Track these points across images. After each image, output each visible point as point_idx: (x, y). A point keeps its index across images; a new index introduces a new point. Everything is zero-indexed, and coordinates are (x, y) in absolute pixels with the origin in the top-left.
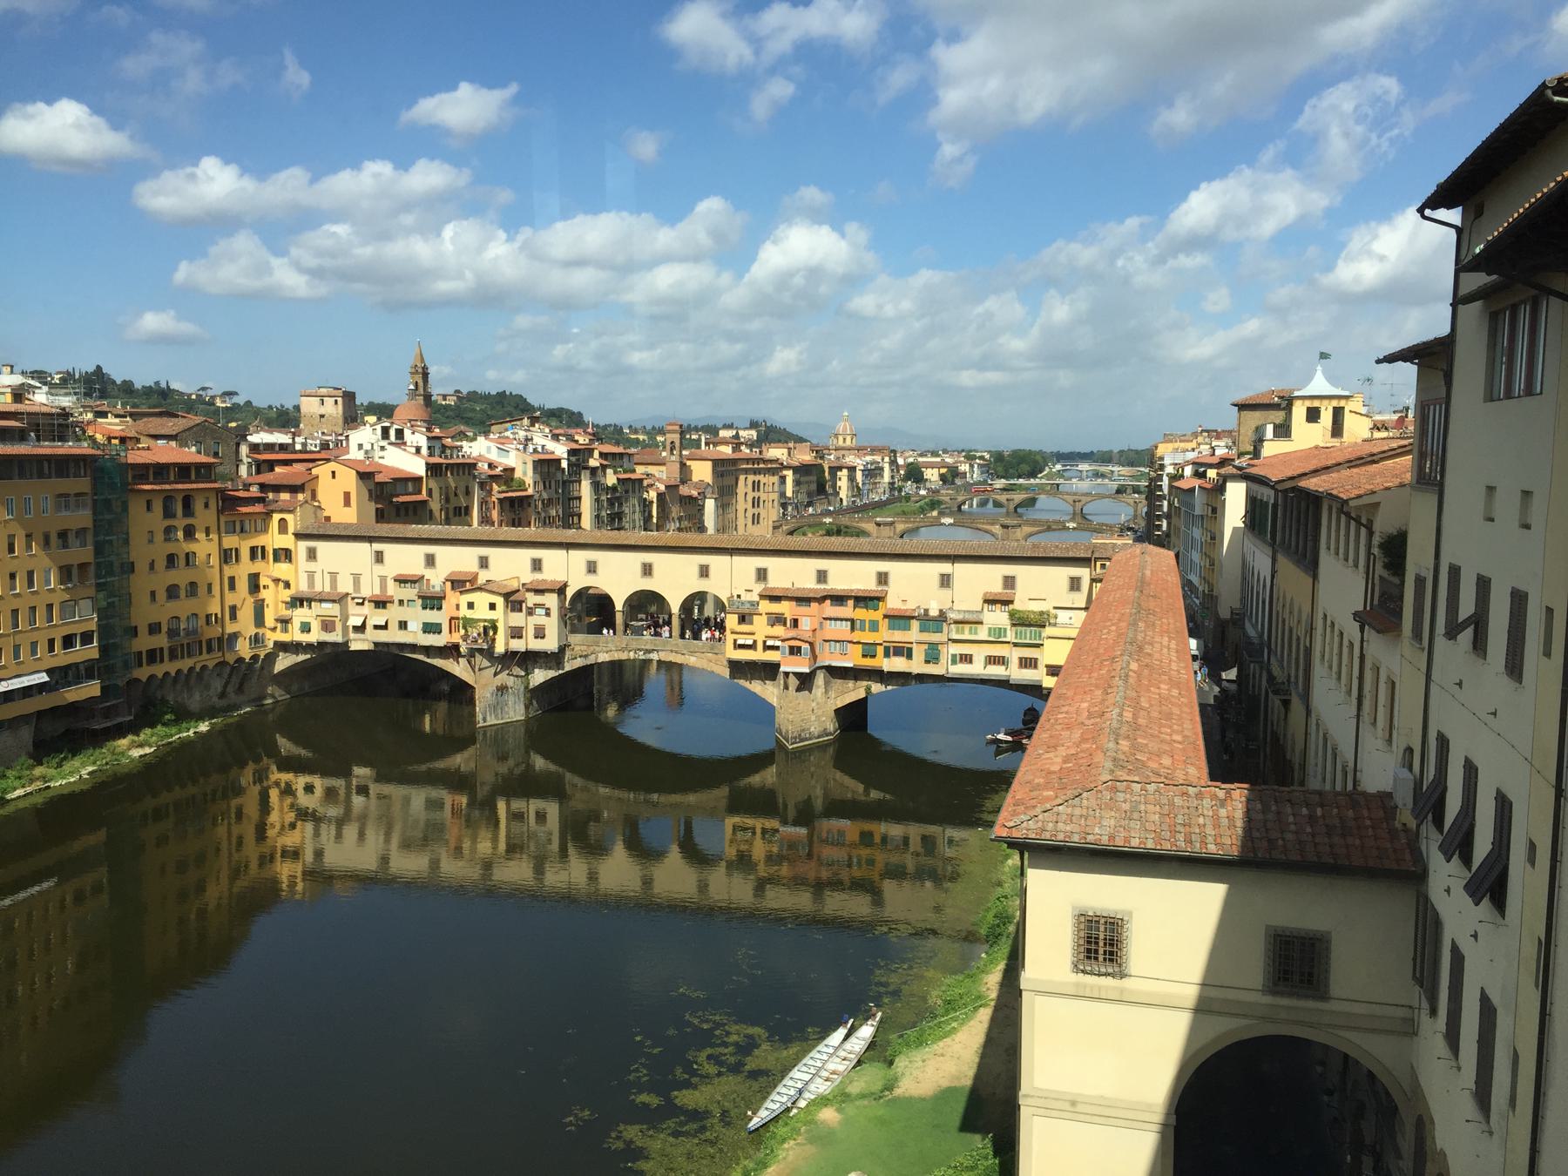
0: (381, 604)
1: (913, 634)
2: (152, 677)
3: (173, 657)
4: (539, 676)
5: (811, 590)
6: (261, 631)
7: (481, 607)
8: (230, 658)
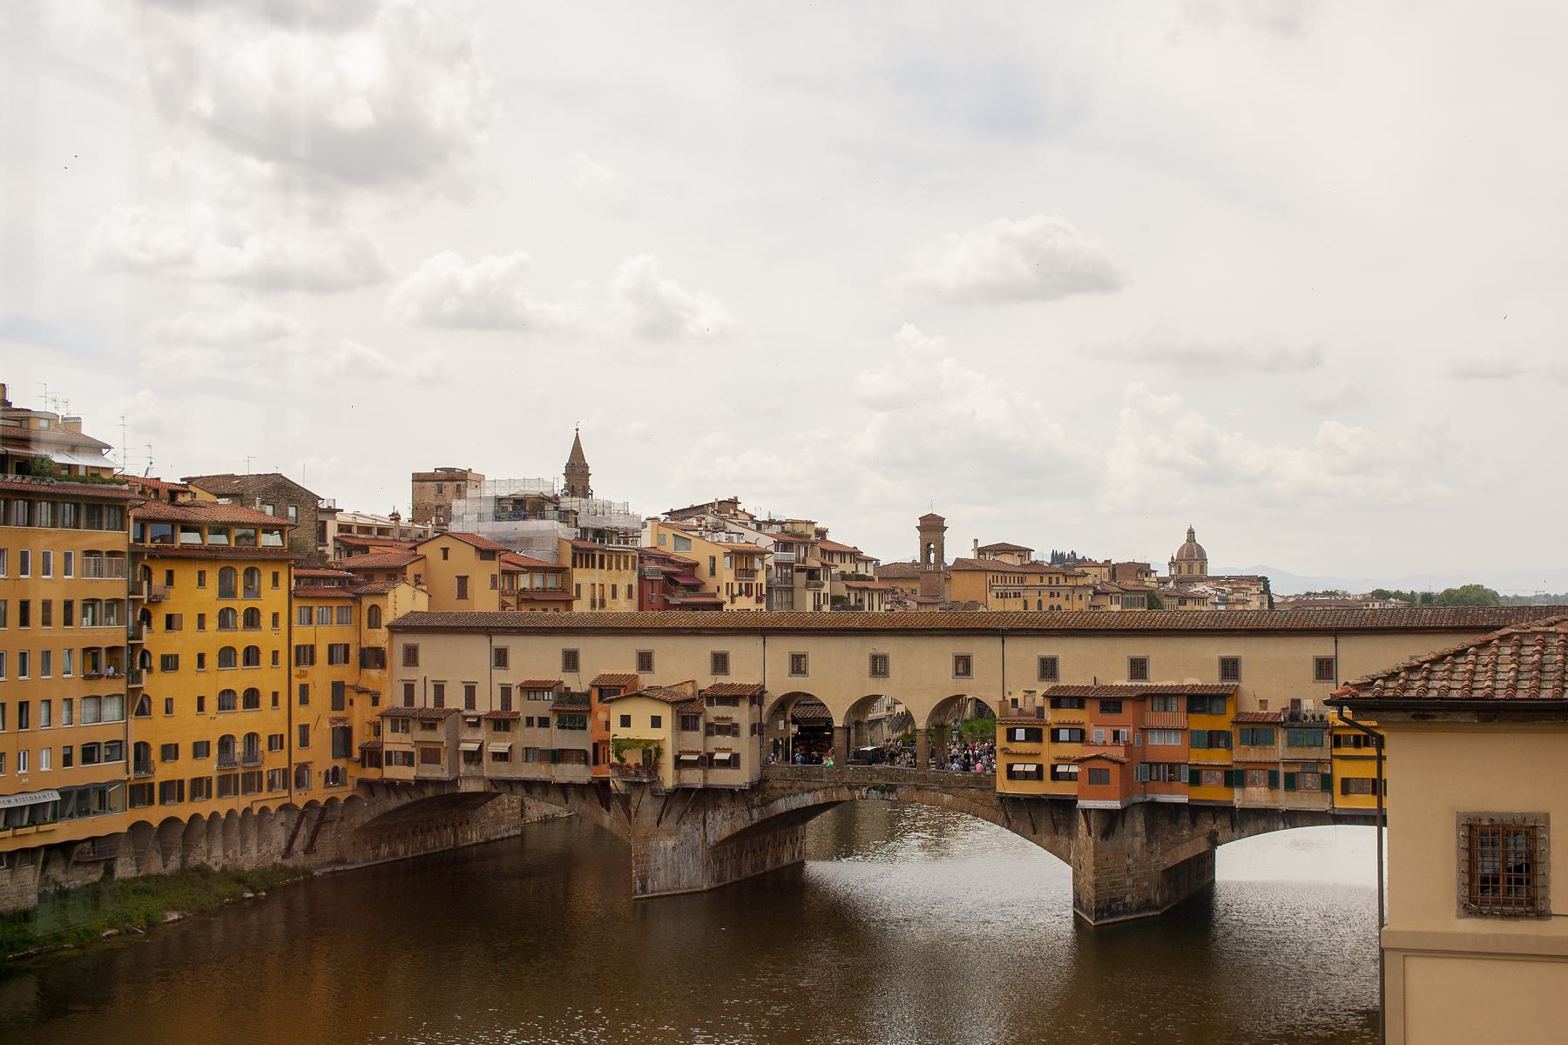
0: (502, 723)
1: (1280, 750)
2: (195, 818)
3: (221, 794)
4: (721, 824)
5: (1121, 688)
6: (341, 764)
7: (641, 723)
8: (300, 799)
